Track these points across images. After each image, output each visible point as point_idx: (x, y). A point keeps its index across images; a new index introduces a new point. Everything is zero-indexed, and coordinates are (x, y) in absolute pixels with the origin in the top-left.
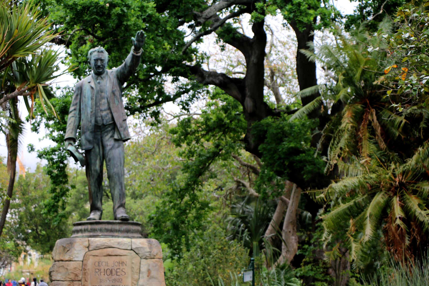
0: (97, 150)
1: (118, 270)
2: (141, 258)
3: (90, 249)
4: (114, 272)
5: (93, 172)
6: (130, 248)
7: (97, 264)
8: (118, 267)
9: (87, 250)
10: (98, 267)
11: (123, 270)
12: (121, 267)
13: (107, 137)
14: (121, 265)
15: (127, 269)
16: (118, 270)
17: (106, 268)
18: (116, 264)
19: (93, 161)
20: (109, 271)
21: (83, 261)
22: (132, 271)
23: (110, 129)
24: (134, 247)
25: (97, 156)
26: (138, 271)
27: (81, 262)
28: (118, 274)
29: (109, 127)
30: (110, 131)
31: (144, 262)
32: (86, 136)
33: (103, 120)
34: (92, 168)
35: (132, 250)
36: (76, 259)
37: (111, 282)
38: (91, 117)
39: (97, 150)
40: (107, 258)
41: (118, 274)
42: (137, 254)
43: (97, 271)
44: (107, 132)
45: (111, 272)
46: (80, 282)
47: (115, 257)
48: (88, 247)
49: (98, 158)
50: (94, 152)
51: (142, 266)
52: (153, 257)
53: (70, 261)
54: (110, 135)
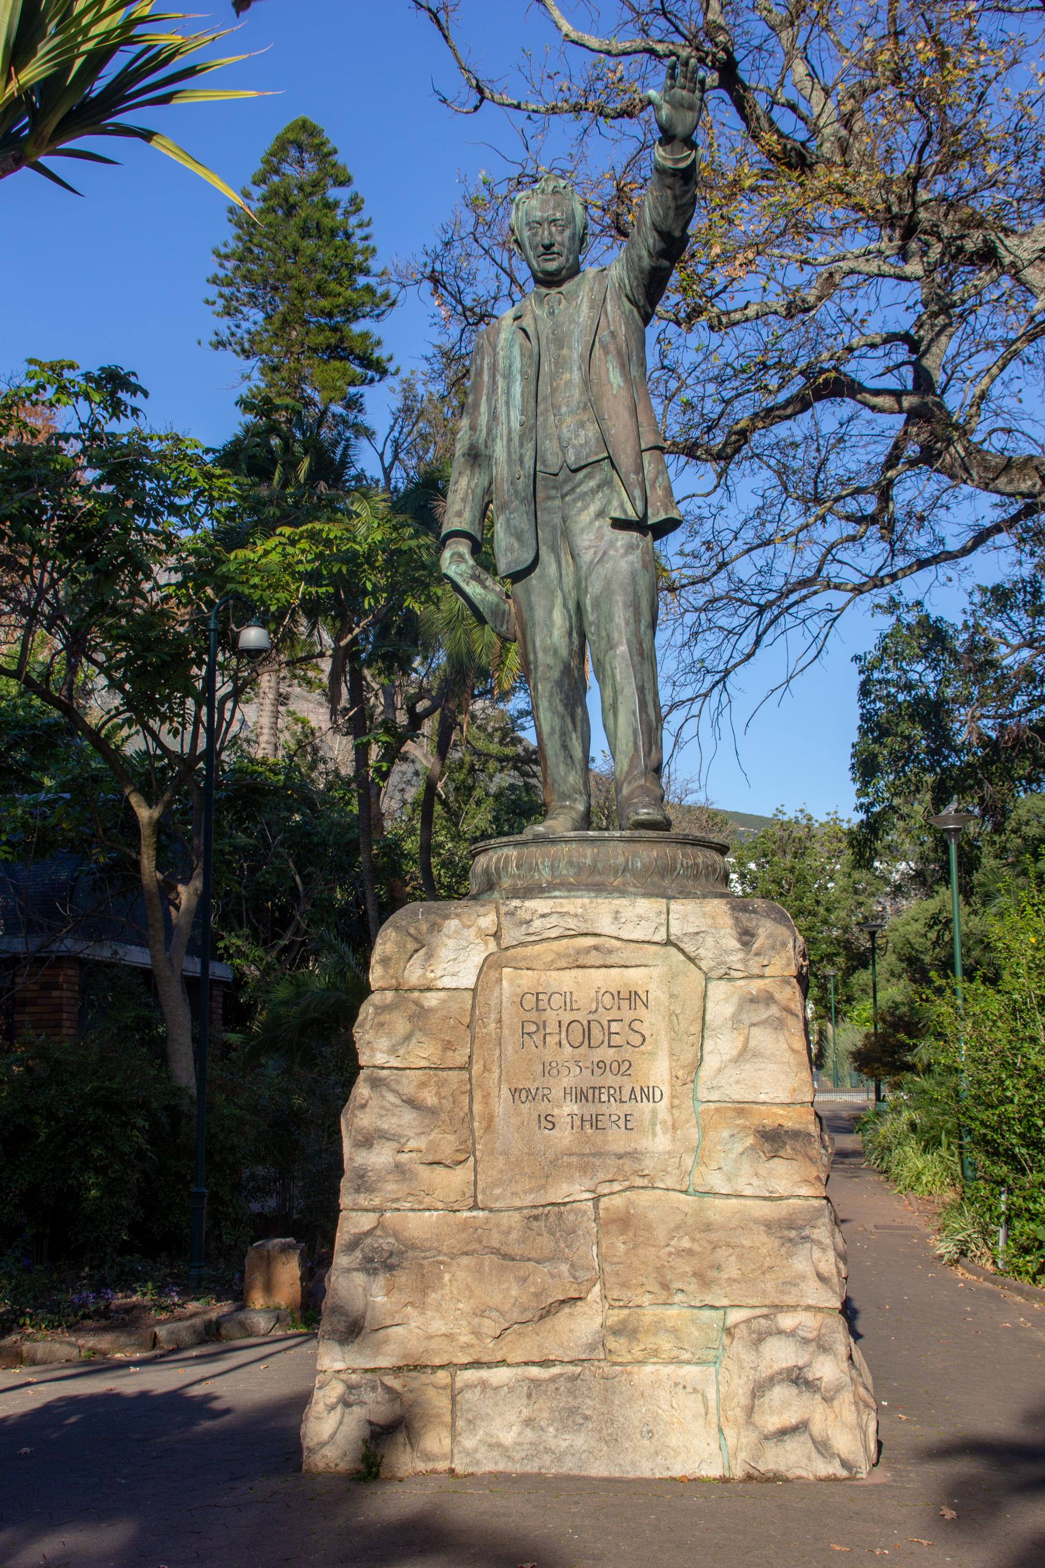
0: (552, 569)
1: (615, 1027)
2: (708, 979)
3: (505, 943)
4: (597, 1033)
5: (540, 655)
6: (660, 936)
7: (530, 1000)
8: (613, 1014)
9: (492, 946)
10: (533, 1016)
11: (636, 1025)
12: (628, 1015)
13: (586, 517)
14: (625, 1004)
15: (652, 1021)
16: (615, 1027)
17: (567, 1017)
18: (607, 998)
19: (539, 614)
20: (576, 1027)
21: (474, 990)
22: (673, 1029)
23: (592, 483)
24: (676, 929)
25: (553, 592)
26: (696, 1028)
27: (468, 996)
28: (616, 1040)
29: (589, 476)
30: (594, 492)
31: (718, 990)
32: (508, 520)
33: (563, 449)
34: (538, 644)
35: (668, 943)
36: (447, 982)
37: (587, 1073)
38: (521, 445)
39: (552, 569)
40: (566, 980)
41: (616, 1040)
42: (689, 958)
43: (533, 1028)
44: (583, 496)
45: (587, 1033)
46: (465, 1075)
47: (604, 970)
48: (497, 935)
49: (559, 601)
50: (542, 577)
51: (710, 1005)
52: (756, 971)
53: (429, 989)
54: (593, 509)
